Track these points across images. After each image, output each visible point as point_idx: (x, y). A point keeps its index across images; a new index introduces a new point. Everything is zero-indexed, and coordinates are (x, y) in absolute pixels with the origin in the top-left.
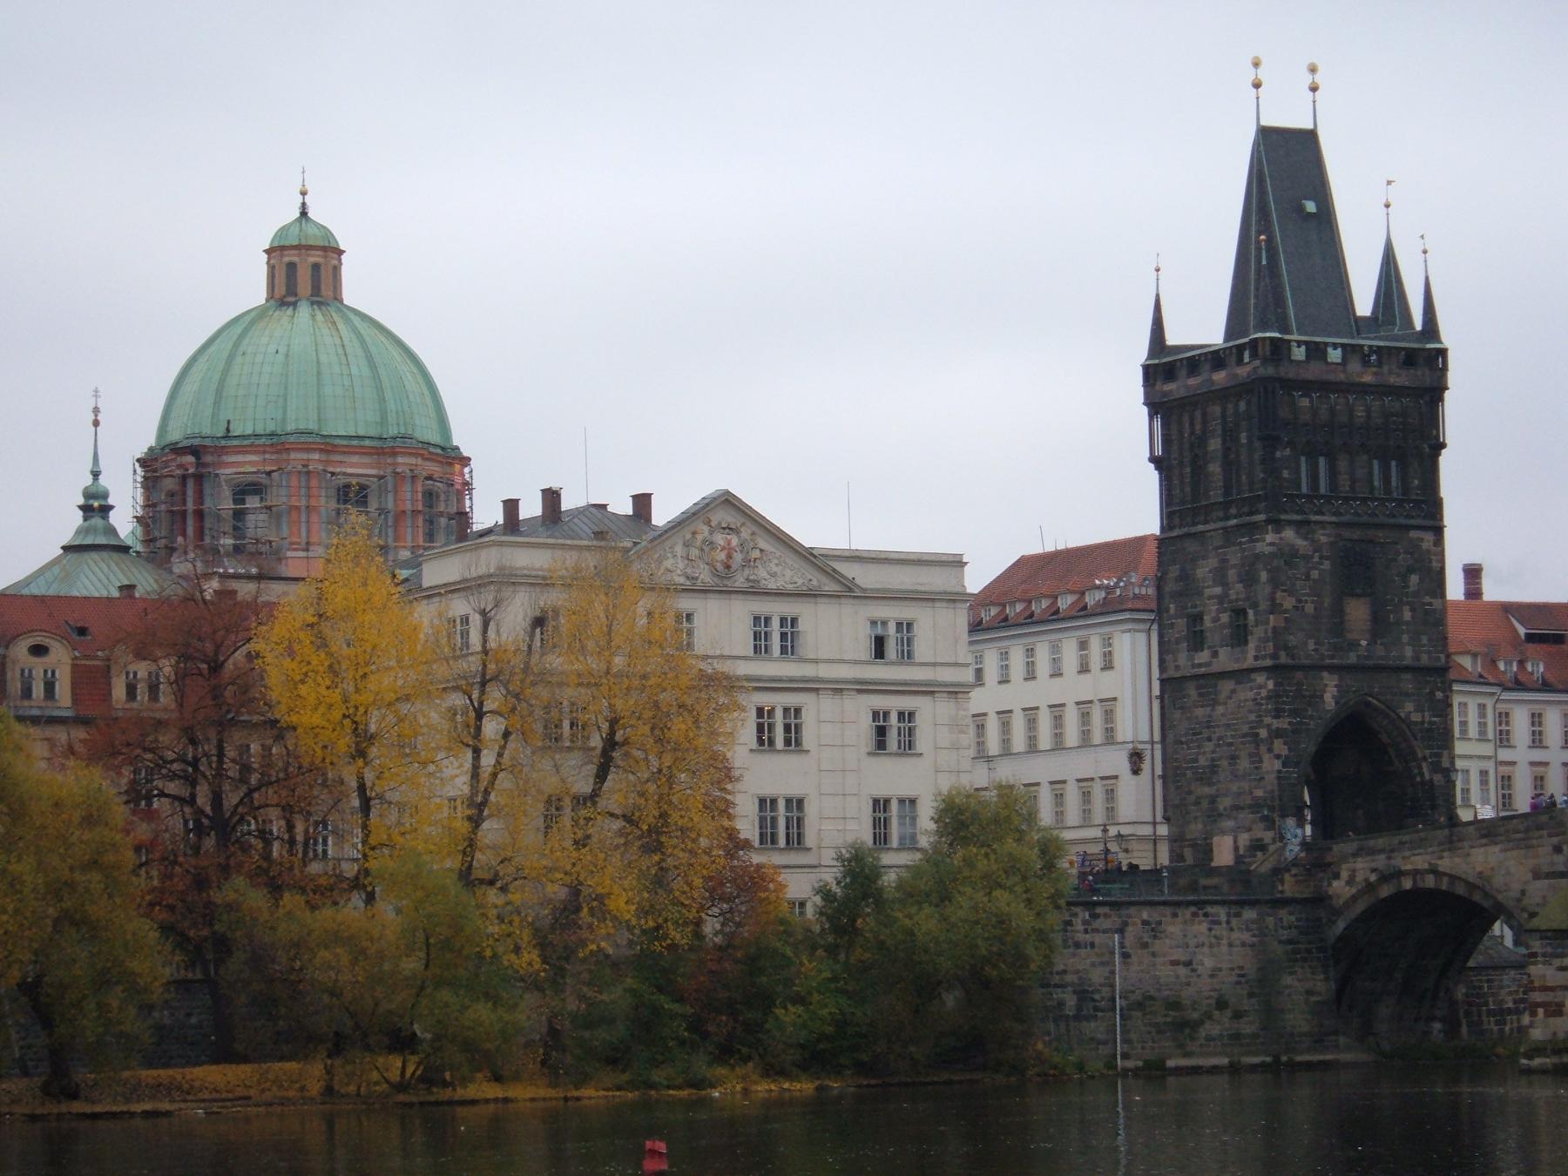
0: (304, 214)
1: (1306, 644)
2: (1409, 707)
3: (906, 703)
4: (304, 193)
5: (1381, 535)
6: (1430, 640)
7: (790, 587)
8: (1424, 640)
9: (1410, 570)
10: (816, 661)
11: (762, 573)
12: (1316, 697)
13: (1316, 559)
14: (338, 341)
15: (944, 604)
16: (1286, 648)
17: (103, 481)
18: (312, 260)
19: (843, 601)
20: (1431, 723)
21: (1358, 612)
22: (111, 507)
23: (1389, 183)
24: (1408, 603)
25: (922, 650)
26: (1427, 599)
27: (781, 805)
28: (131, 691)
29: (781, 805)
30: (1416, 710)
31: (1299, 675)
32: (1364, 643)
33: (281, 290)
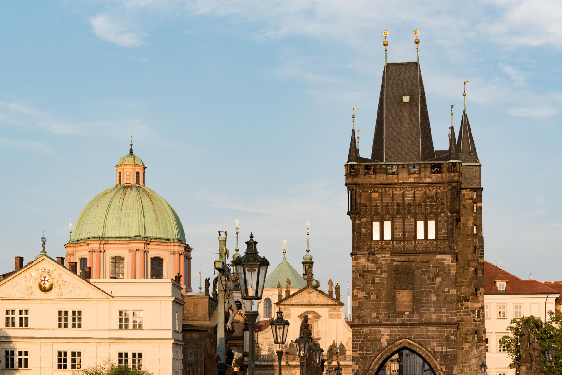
1: (371, 314)
2: (434, 344)
5: (419, 258)
6: (448, 310)
7: (79, 297)
8: (444, 310)
9: (436, 275)
10: (90, 330)
11: (64, 290)
13: (379, 272)
14: (121, 200)
15: (159, 302)
16: (359, 317)
20: (447, 352)
21: (404, 298)
24: (434, 292)
26: (447, 290)
31: (366, 330)
32: (407, 313)
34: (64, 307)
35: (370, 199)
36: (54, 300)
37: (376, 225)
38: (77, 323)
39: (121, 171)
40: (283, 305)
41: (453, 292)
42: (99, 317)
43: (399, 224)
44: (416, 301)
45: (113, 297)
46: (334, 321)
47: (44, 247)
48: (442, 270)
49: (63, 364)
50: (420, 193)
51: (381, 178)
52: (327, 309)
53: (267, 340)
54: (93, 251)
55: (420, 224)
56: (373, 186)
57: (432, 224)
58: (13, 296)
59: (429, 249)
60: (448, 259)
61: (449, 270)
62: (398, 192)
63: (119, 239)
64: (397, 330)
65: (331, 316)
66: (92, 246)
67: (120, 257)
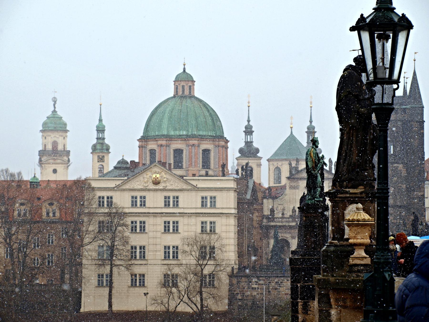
0: (184, 70)
3: (212, 219)
4: (184, 65)
7: (176, 188)
10: (184, 208)
11: (168, 184)
17: (313, 124)
18: (182, 84)
19: (192, 191)
22: (316, 132)
23: (415, 53)
25: (218, 204)
27: (171, 248)
28: (48, 214)
29: (171, 248)
30: (394, 219)
33: (180, 93)
36: (161, 190)
39: (177, 84)
40: (294, 178)
42: (190, 201)
45: (198, 188)
47: (55, 107)
49: (166, 230)
53: (280, 206)
54: (161, 146)
58: (136, 187)
61: (401, 173)
63: (180, 137)
66: (160, 142)
67: (179, 149)
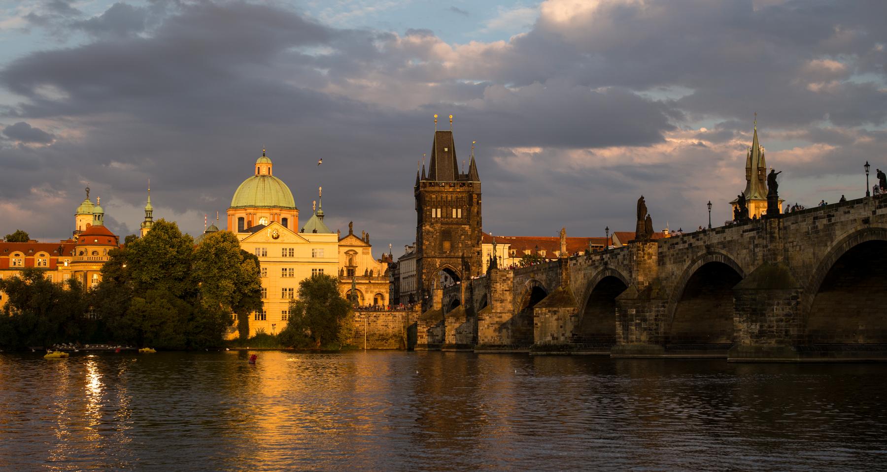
12: (434, 265)
21: (447, 245)
34: (285, 246)
35: (431, 198)
37: (434, 210)
38: (292, 254)
41: (469, 243)
43: (444, 210)
44: (452, 247)
46: (365, 256)
48: (464, 232)
50: (454, 196)
51: (437, 188)
52: (361, 249)
55: (454, 211)
56: (433, 192)
57: (459, 211)
59: (458, 223)
60: (467, 227)
62: (444, 195)
64: (444, 260)
65: (363, 253)
